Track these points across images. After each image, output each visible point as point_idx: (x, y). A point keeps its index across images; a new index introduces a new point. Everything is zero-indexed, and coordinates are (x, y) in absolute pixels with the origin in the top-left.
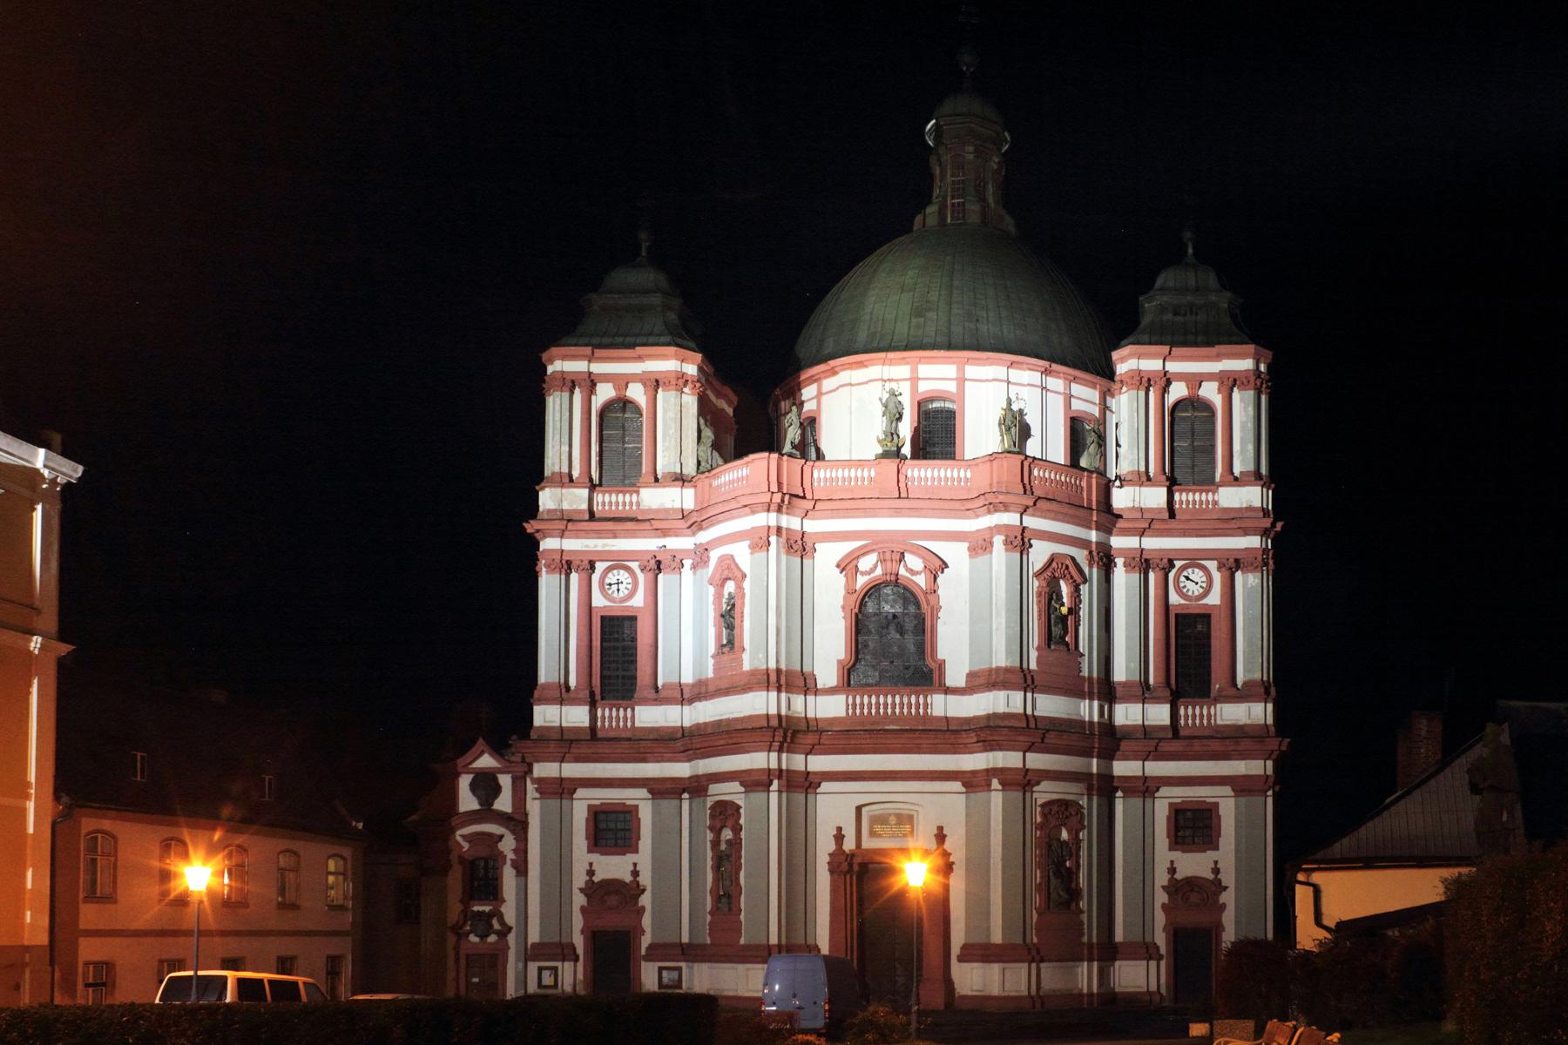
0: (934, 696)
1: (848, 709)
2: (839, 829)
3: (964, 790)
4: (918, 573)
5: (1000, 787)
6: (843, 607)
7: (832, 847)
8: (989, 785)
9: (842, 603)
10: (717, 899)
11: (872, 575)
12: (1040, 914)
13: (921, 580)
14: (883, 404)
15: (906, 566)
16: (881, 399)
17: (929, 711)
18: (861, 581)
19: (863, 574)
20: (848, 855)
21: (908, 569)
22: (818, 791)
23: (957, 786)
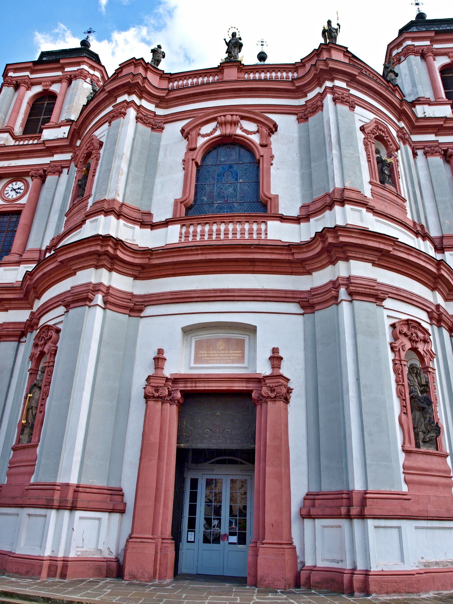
0: (269, 223)
1: (180, 237)
2: (160, 351)
3: (302, 311)
4: (254, 133)
5: (349, 299)
6: (184, 161)
7: (151, 372)
8: (336, 297)
9: (183, 158)
10: (22, 428)
11: (212, 136)
12: (407, 452)
13: (256, 138)
14: (227, 44)
15: (241, 128)
16: (225, 40)
17: (263, 236)
18: (201, 141)
19: (203, 136)
20: (167, 379)
21: (245, 131)
22: (142, 315)
23: (293, 308)
